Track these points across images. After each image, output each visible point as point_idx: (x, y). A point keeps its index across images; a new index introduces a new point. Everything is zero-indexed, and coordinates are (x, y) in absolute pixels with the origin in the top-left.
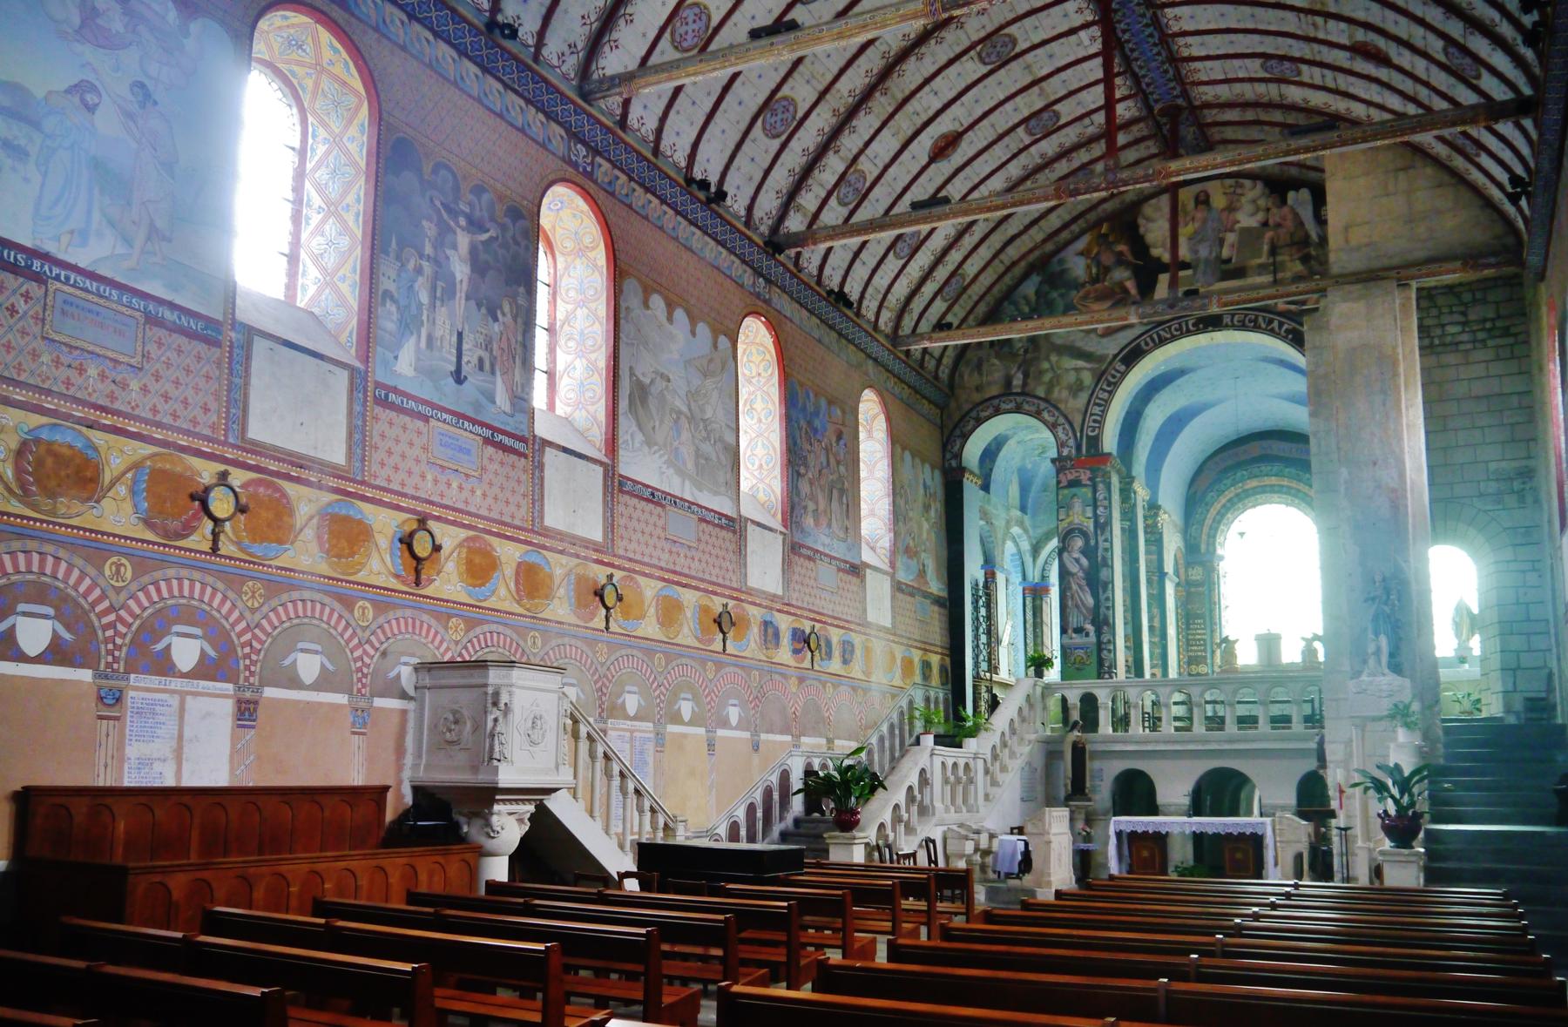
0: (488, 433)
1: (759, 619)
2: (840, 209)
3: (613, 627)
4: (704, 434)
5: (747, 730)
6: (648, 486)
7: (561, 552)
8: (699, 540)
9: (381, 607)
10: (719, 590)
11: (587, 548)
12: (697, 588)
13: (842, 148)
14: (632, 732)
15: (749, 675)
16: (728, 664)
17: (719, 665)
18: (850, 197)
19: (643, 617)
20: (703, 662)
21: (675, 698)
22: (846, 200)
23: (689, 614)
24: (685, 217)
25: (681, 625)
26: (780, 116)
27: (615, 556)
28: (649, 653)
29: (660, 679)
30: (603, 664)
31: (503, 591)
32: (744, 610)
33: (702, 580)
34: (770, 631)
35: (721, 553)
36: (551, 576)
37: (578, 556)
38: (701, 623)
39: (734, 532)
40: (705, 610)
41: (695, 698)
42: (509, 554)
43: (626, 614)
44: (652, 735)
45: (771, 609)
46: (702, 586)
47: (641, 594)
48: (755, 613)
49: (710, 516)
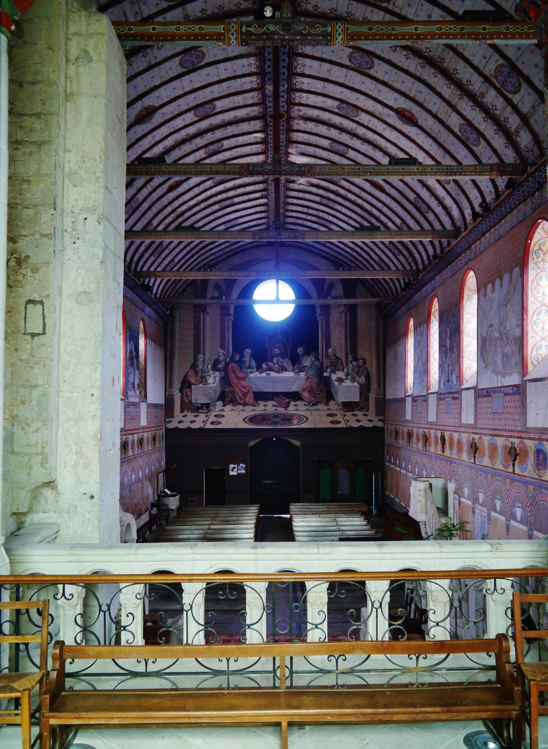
0: (451, 395)
1: (533, 449)
2: (522, 91)
3: (477, 462)
4: (506, 342)
5: (525, 525)
6: (485, 389)
7: (464, 432)
8: (504, 407)
9: (440, 460)
10: (512, 434)
11: (470, 428)
12: (502, 436)
13: (481, 90)
14: (481, 511)
15: (527, 489)
16: (517, 481)
17: (512, 481)
18: (514, 80)
19: (484, 456)
20: (506, 477)
21: (494, 499)
22: (517, 85)
23: (500, 452)
24: (497, 223)
25: (497, 458)
26: (469, 134)
27: (477, 428)
28: (486, 472)
29: (490, 487)
30: (474, 478)
31: (455, 452)
32: (524, 443)
33: (505, 430)
34: (541, 456)
35: (512, 410)
36: (463, 443)
37: (468, 433)
38: (504, 456)
39: (520, 394)
40: (505, 447)
41: (501, 500)
42: (456, 436)
43: (480, 455)
44: (486, 515)
45: (542, 440)
46: (505, 433)
47: (483, 444)
48: (530, 444)
49: (508, 390)
